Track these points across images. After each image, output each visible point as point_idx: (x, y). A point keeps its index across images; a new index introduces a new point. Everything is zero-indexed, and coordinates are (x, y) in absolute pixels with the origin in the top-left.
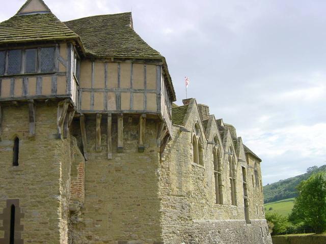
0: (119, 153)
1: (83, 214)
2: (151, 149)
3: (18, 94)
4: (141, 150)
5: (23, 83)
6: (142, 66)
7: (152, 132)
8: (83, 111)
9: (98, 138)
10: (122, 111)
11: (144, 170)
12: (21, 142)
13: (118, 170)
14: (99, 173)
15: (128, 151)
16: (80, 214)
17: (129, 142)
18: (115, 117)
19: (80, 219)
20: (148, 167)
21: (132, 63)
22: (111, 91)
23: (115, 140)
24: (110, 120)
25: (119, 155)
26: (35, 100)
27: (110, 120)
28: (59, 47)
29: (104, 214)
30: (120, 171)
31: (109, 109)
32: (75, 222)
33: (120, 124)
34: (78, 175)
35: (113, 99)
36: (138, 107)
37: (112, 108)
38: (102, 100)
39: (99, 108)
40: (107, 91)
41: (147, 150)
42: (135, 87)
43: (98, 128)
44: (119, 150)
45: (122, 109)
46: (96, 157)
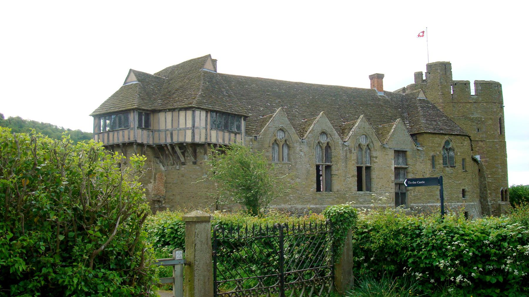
0: (183, 165)
1: (165, 202)
2: (200, 162)
3: (116, 141)
4: (195, 163)
5: (118, 134)
6: (184, 112)
7: (202, 151)
8: (155, 143)
9: (170, 158)
10: (173, 143)
11: (197, 176)
12: (121, 165)
13: (183, 176)
14: (173, 178)
15: (188, 164)
16: (163, 202)
17: (189, 158)
18: (172, 146)
19: (164, 205)
20: (199, 174)
21: (179, 111)
22: (168, 130)
23: (178, 158)
24: (169, 147)
25: (183, 166)
26: (123, 144)
27: (169, 147)
28: (130, 112)
29: (175, 202)
30: (184, 176)
31: (167, 142)
32: (161, 207)
33: (177, 149)
34: (157, 181)
35: (169, 135)
36: (181, 140)
37: (169, 141)
38: (164, 136)
39: (162, 142)
40: (166, 130)
41: (198, 163)
42: (181, 127)
43: (167, 152)
44: (183, 164)
45: (174, 141)
46: (171, 169)
